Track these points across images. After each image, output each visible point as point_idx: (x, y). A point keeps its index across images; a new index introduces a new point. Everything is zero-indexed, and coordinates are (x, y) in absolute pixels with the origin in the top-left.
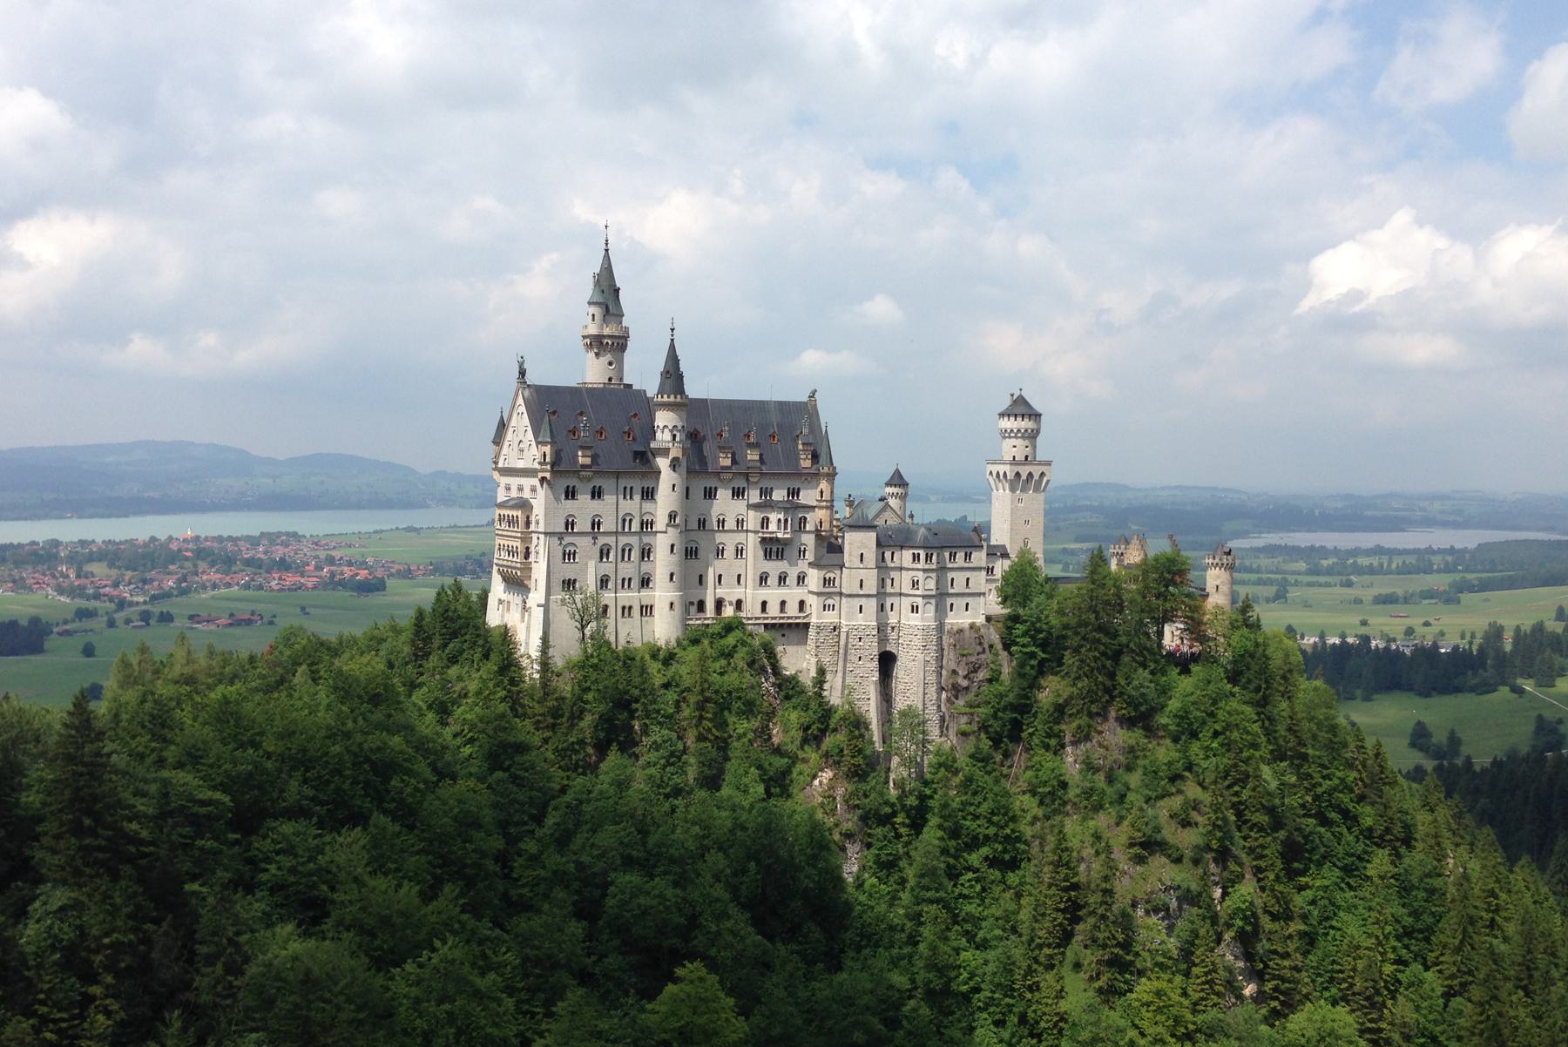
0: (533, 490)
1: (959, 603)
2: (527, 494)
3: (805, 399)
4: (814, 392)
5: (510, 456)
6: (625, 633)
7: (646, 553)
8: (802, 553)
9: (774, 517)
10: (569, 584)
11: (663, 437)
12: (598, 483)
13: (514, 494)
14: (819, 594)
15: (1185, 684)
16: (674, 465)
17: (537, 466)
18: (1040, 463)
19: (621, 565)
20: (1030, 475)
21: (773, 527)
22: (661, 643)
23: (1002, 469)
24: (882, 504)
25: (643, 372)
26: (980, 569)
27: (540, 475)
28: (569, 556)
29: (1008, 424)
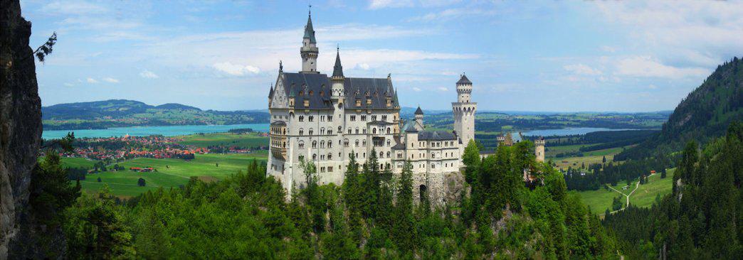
1: (449, 163)
2: (284, 119)
3: (386, 77)
6: (325, 179)
7: (330, 144)
8: (389, 143)
10: (301, 158)
11: (336, 94)
15: (533, 194)
16: (340, 106)
17: (290, 108)
21: (377, 132)
27: (290, 111)
28: (301, 145)
29: (461, 87)
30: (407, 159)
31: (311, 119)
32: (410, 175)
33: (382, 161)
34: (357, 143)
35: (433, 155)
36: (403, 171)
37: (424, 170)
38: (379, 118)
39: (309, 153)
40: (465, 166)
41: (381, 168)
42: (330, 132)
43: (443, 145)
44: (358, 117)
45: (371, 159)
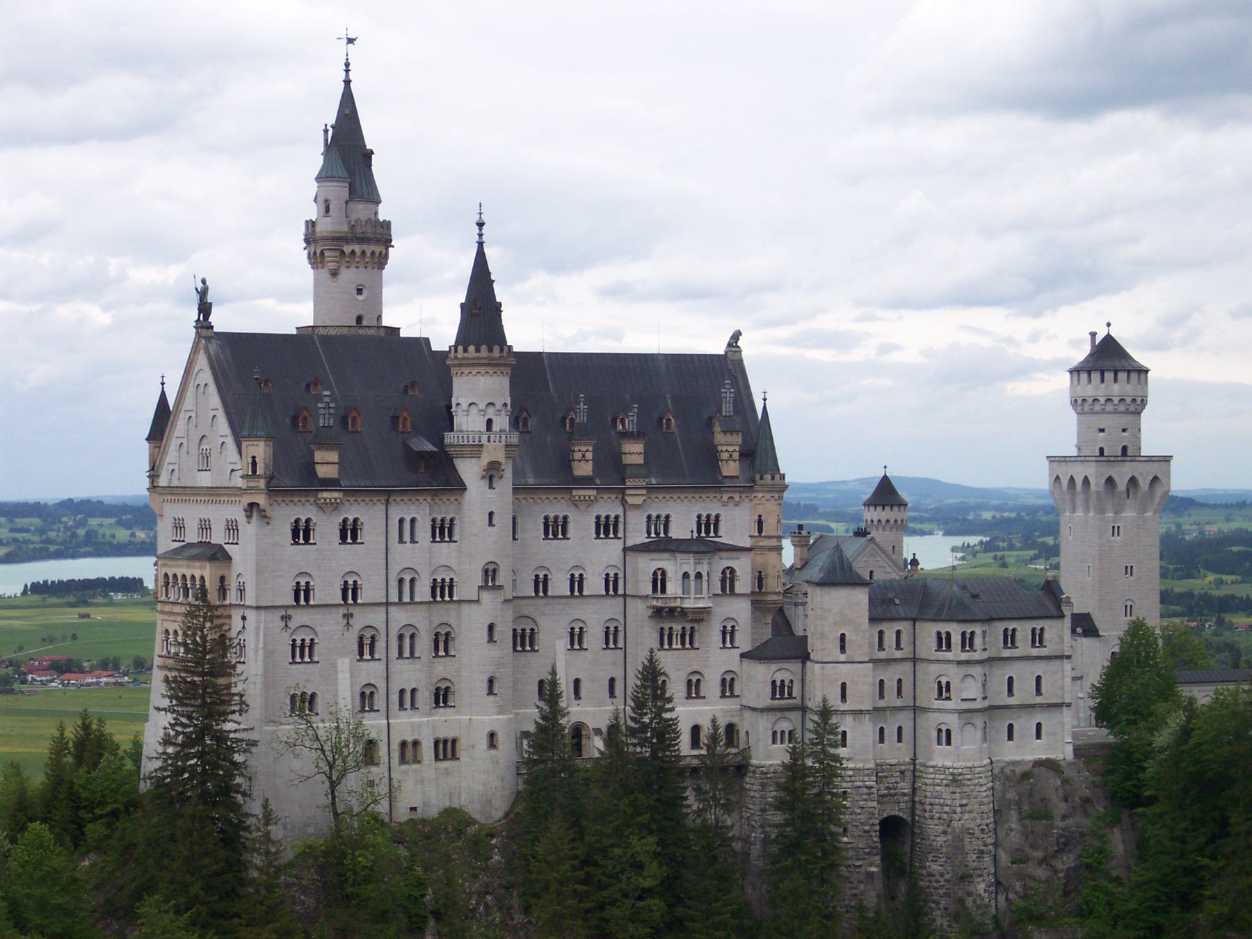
0: (232, 528)
1: (1025, 725)
2: (218, 537)
3: (720, 350)
4: (736, 336)
5: (180, 462)
7: (443, 642)
8: (728, 635)
9: (674, 566)
10: (303, 704)
11: (468, 423)
12: (352, 512)
13: (192, 536)
14: (762, 710)
16: (491, 474)
17: (240, 483)
18: (1151, 459)
19: (396, 666)
20: (1133, 481)
21: (673, 588)
22: (475, 811)
23: (1079, 472)
24: (862, 540)
25: (422, 309)
26: (1061, 657)
27: (246, 500)
28: (303, 650)
29: (1093, 388)
30: (814, 703)
31: (350, 532)
32: (830, 769)
33: (686, 714)
34: (576, 638)
35: (944, 690)
36: (794, 754)
37: (897, 754)
38: (682, 528)
39: (341, 680)
40: (1111, 739)
41: (695, 742)
42: (442, 589)
43: (988, 638)
44: (582, 524)
45: (639, 705)
